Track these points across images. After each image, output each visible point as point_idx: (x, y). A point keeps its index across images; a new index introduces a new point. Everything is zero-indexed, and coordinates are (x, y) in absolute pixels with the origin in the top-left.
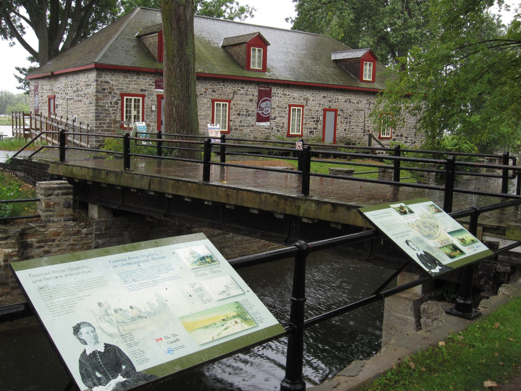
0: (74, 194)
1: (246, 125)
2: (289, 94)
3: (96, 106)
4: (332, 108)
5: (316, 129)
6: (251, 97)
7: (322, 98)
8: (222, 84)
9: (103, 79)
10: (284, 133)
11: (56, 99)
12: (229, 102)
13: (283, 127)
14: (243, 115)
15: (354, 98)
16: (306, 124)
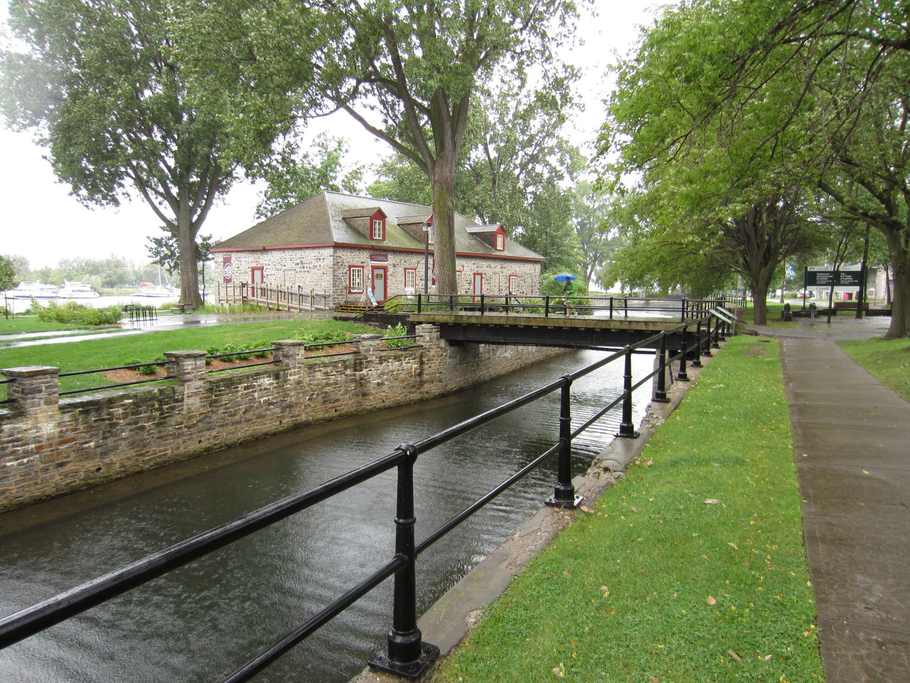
9: (337, 255)
12: (415, 269)
15: (493, 264)
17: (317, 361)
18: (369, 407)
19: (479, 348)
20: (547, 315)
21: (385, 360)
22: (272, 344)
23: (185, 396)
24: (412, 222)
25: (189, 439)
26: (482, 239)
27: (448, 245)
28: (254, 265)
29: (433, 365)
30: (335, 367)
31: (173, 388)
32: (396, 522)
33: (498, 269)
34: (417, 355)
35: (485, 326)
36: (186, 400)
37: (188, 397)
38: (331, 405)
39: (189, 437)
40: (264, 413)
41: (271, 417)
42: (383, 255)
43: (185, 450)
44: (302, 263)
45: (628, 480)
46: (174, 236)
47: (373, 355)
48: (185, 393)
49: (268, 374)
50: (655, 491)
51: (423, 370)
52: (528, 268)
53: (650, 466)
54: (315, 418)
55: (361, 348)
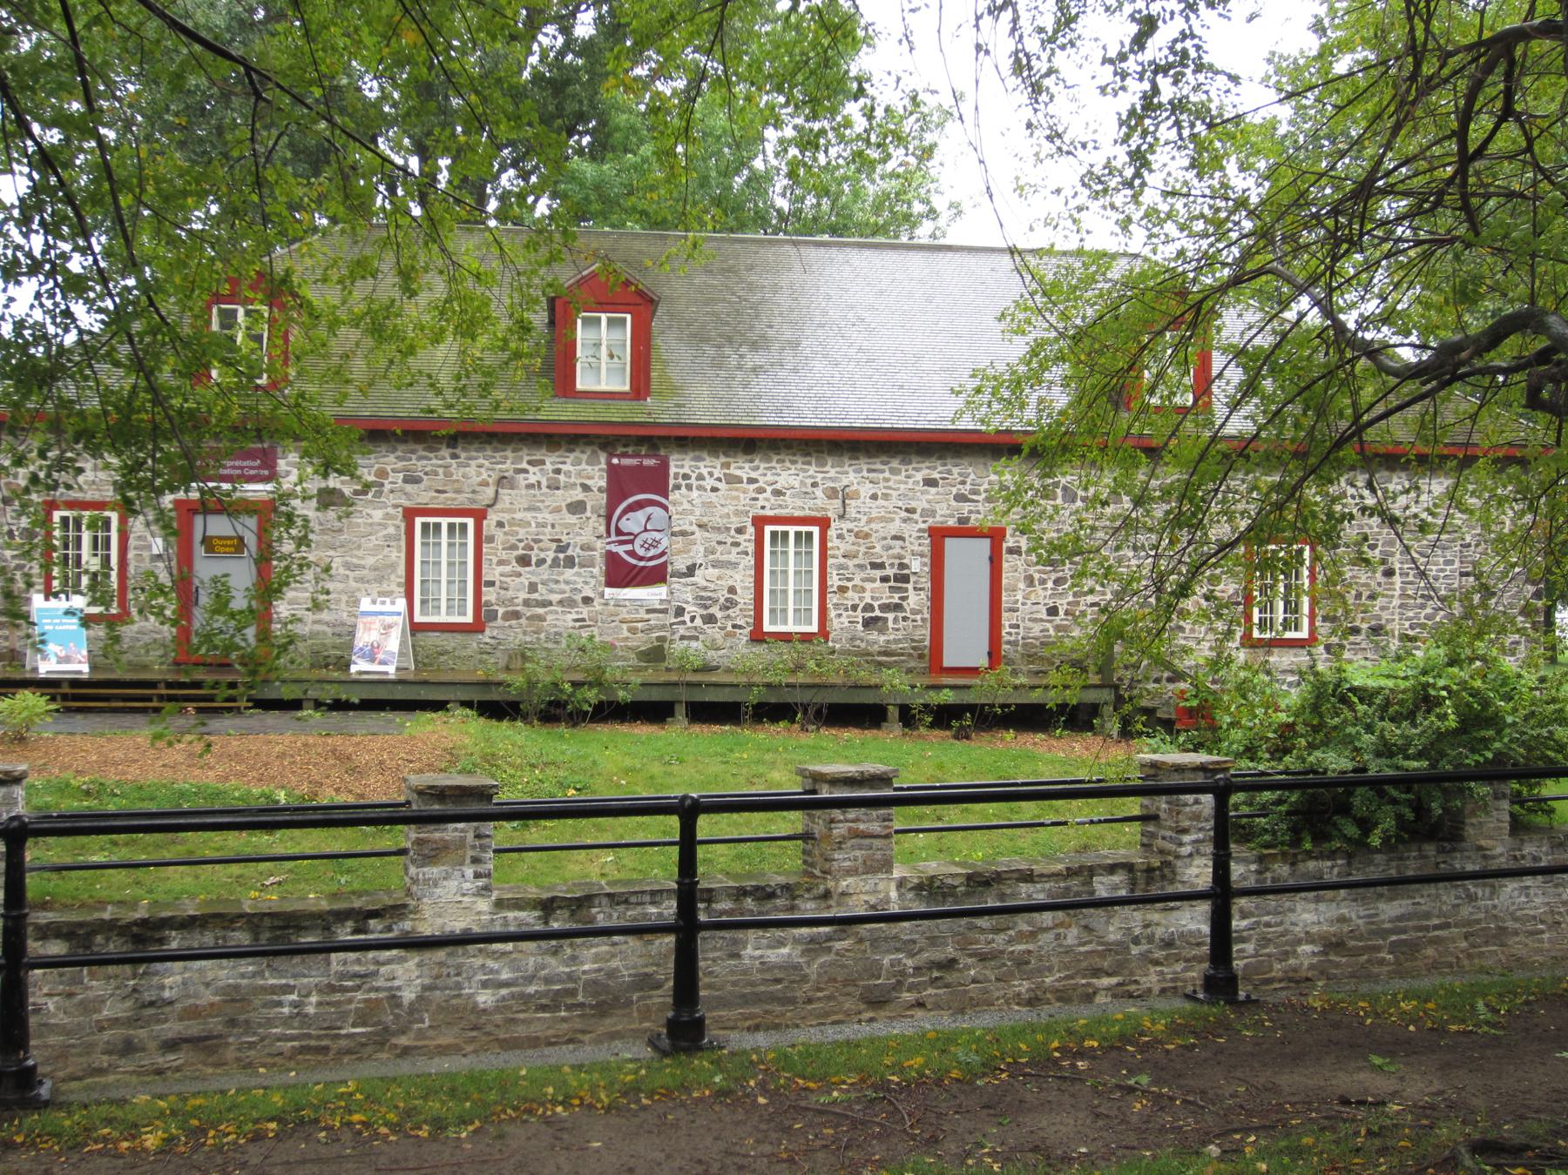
1: (555, 598)
2: (754, 475)
4: (972, 523)
5: (886, 608)
6: (578, 494)
7: (920, 487)
8: (445, 452)
10: (734, 626)
12: (480, 515)
13: (730, 604)
14: (541, 562)
16: (842, 589)
42: (250, 455)
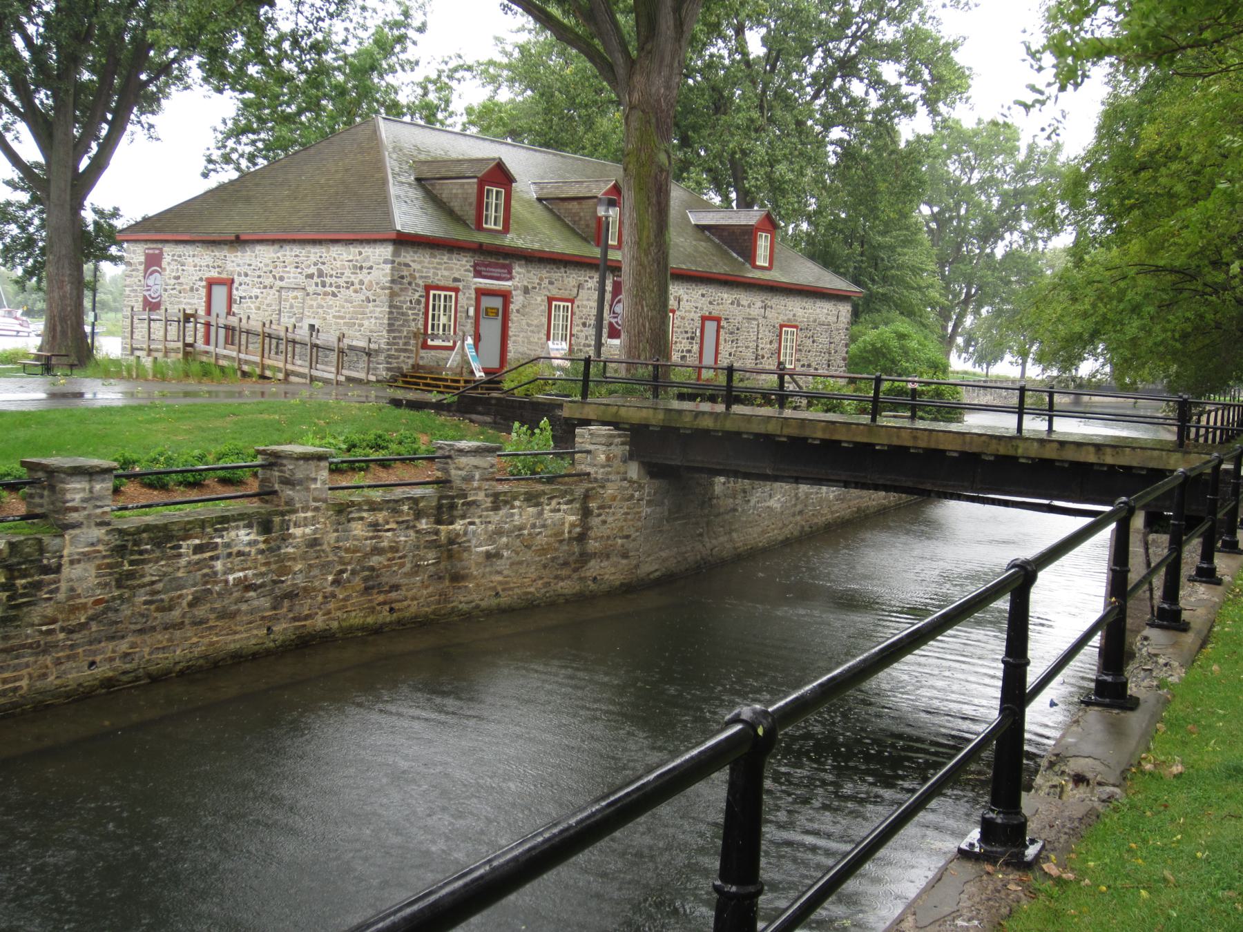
0: (631, 444)
3: (390, 307)
5: (689, 351)
9: (401, 259)
11: (236, 285)
12: (572, 301)
15: (745, 298)
17: (356, 497)
18: (463, 607)
19: (712, 484)
20: (874, 420)
21: (506, 502)
22: (259, 452)
23: (65, 560)
24: (571, 194)
25: (69, 658)
26: (720, 238)
27: (653, 250)
28: (214, 274)
29: (610, 519)
30: (396, 511)
31: (40, 541)
32: (716, 888)
33: (756, 311)
34: (577, 495)
35: (733, 437)
36: (66, 570)
37: (72, 562)
38: (381, 598)
39: (68, 652)
40: (234, 608)
41: (250, 618)
42: (503, 266)
43: (58, 682)
44: (321, 274)
45: (1132, 807)
46: (35, 200)
47: (479, 488)
48: (65, 552)
49: (246, 519)
50: (1206, 834)
51: (590, 528)
52: (823, 310)
53: (1178, 776)
54: (344, 624)
55: (453, 472)
